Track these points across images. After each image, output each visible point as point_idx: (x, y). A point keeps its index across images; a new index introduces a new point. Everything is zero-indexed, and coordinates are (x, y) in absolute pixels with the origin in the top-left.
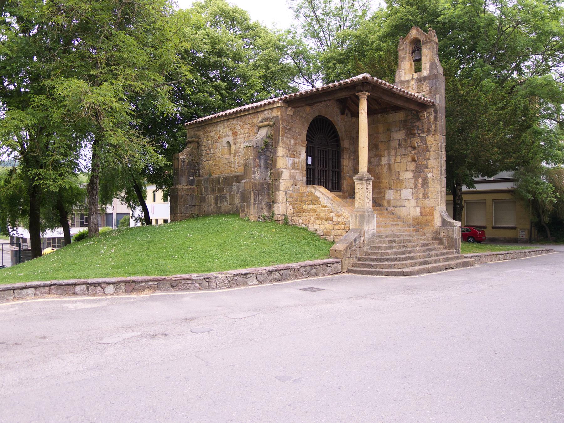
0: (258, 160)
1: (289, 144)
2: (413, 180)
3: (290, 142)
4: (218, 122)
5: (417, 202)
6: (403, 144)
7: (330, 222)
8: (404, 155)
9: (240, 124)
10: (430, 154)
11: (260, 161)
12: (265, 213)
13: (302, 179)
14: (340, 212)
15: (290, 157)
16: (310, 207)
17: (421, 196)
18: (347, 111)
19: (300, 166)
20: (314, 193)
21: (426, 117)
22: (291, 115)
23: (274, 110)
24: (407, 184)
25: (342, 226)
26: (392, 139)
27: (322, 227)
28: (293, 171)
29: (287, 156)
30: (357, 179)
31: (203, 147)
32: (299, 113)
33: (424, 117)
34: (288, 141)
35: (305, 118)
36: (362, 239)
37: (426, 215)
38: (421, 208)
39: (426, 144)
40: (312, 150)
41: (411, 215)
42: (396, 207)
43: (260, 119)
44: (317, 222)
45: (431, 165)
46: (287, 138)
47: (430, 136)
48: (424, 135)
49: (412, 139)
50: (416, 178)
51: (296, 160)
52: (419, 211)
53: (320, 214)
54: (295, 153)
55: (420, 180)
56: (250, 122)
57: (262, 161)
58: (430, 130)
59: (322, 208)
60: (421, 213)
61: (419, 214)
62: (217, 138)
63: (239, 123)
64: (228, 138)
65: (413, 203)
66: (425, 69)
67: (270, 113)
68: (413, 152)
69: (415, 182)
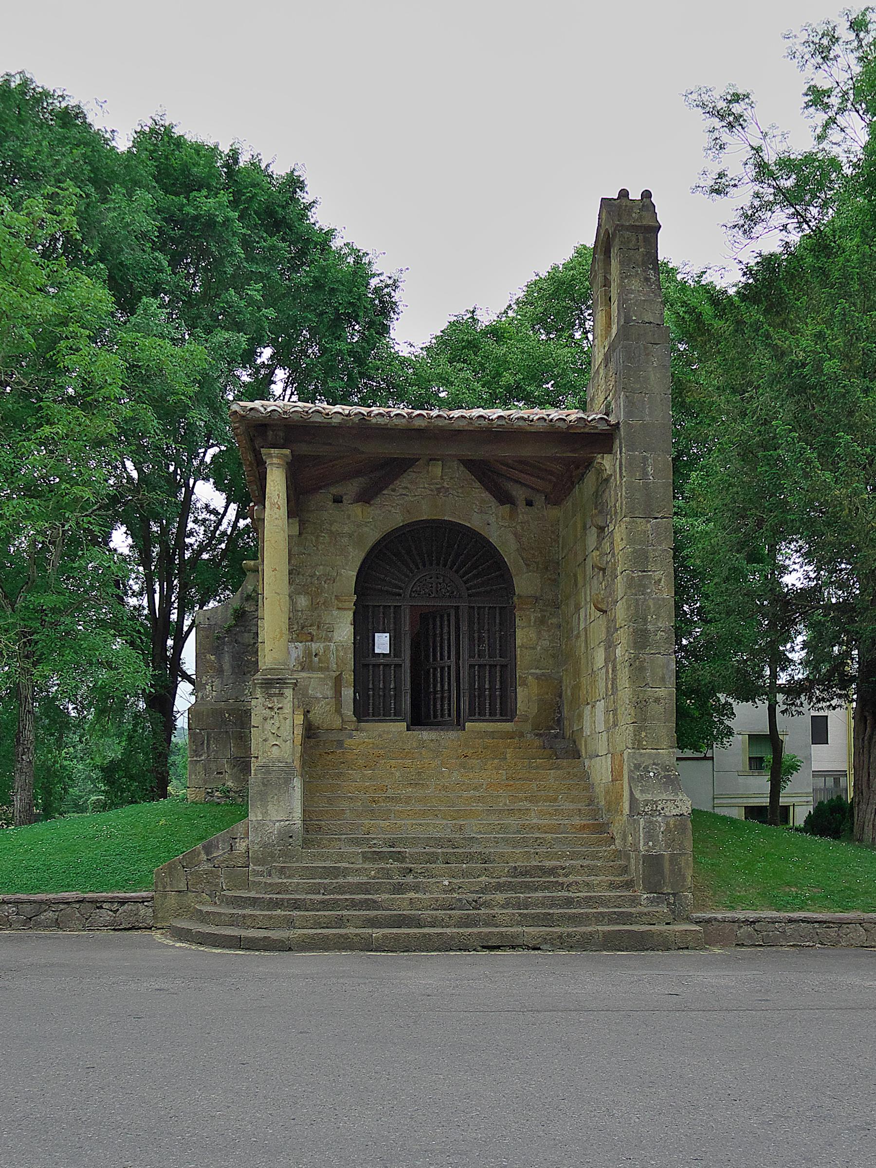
0: (213, 657)
11: (219, 658)
12: (230, 784)
18: (519, 493)
19: (333, 659)
28: (304, 674)
35: (350, 536)
36: (241, 846)
51: (314, 646)
54: (313, 630)
57: (227, 658)
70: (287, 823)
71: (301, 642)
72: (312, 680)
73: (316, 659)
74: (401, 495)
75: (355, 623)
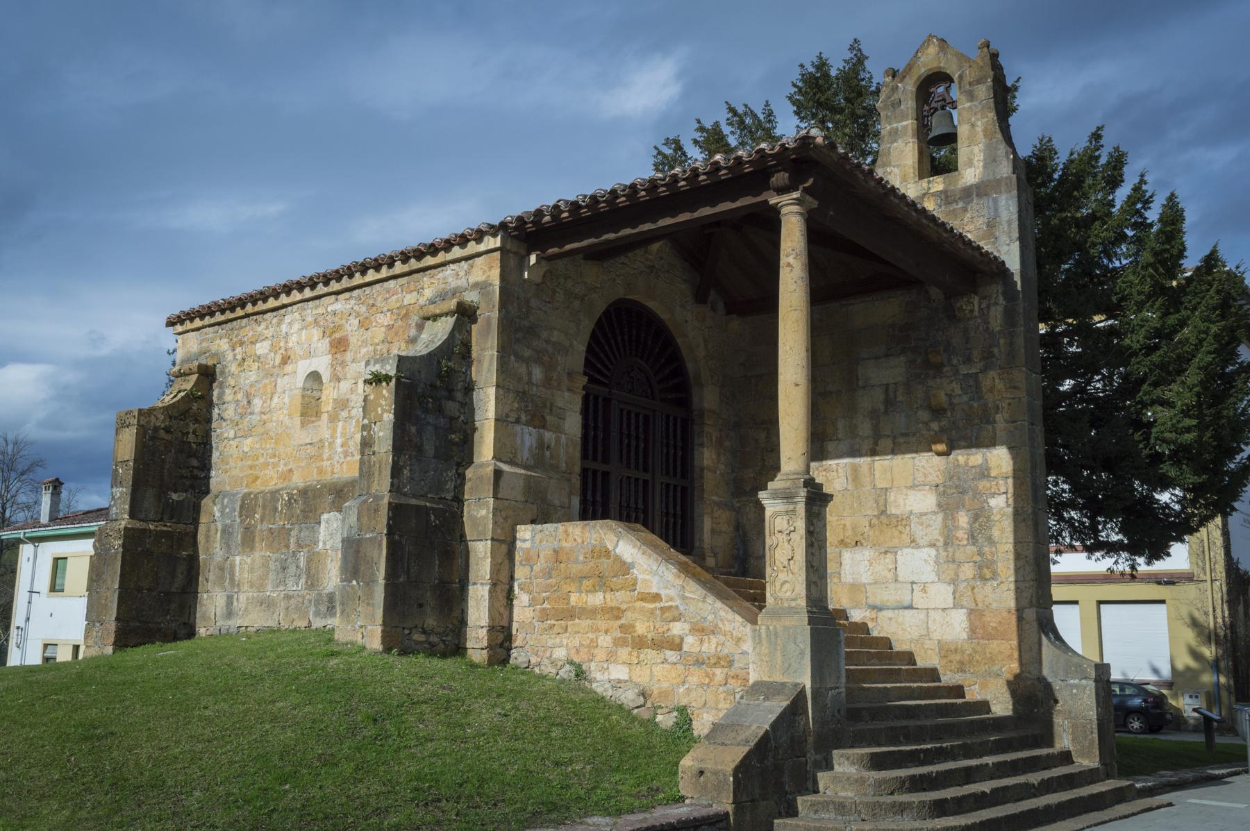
1: (525, 378)
2: (940, 517)
3: (530, 374)
4: (284, 306)
5: (954, 593)
6: (900, 398)
7: (671, 655)
8: (905, 435)
9: (358, 315)
10: (994, 429)
13: (566, 501)
14: (710, 618)
15: (528, 424)
16: (597, 599)
17: (968, 571)
18: (713, 295)
20: (611, 548)
21: (976, 313)
22: (538, 285)
23: (479, 261)
24: (918, 531)
25: (718, 671)
26: (861, 383)
27: (642, 676)
29: (518, 421)
30: (775, 495)
31: (228, 391)
32: (562, 280)
33: (972, 311)
34: (523, 370)
37: (990, 637)
38: (971, 612)
39: (980, 398)
40: (600, 406)
41: (936, 636)
42: (880, 609)
43: (428, 293)
44: (623, 653)
45: (999, 466)
46: (519, 358)
47: (992, 373)
48: (974, 371)
49: (930, 383)
50: (947, 508)
51: (548, 435)
52: (966, 624)
53: (633, 626)
55: (963, 519)
56: (393, 302)
58: (991, 355)
59: (639, 604)
60: (973, 630)
61: (964, 636)
62: (278, 360)
63: (356, 308)
64: (315, 360)
65: (942, 594)
66: (970, 164)
67: (462, 274)
68: (935, 426)
69: (946, 526)
70: (837, 690)
71: (535, 428)
72: (552, 481)
73: (548, 453)
74: (623, 263)
75: (585, 412)
